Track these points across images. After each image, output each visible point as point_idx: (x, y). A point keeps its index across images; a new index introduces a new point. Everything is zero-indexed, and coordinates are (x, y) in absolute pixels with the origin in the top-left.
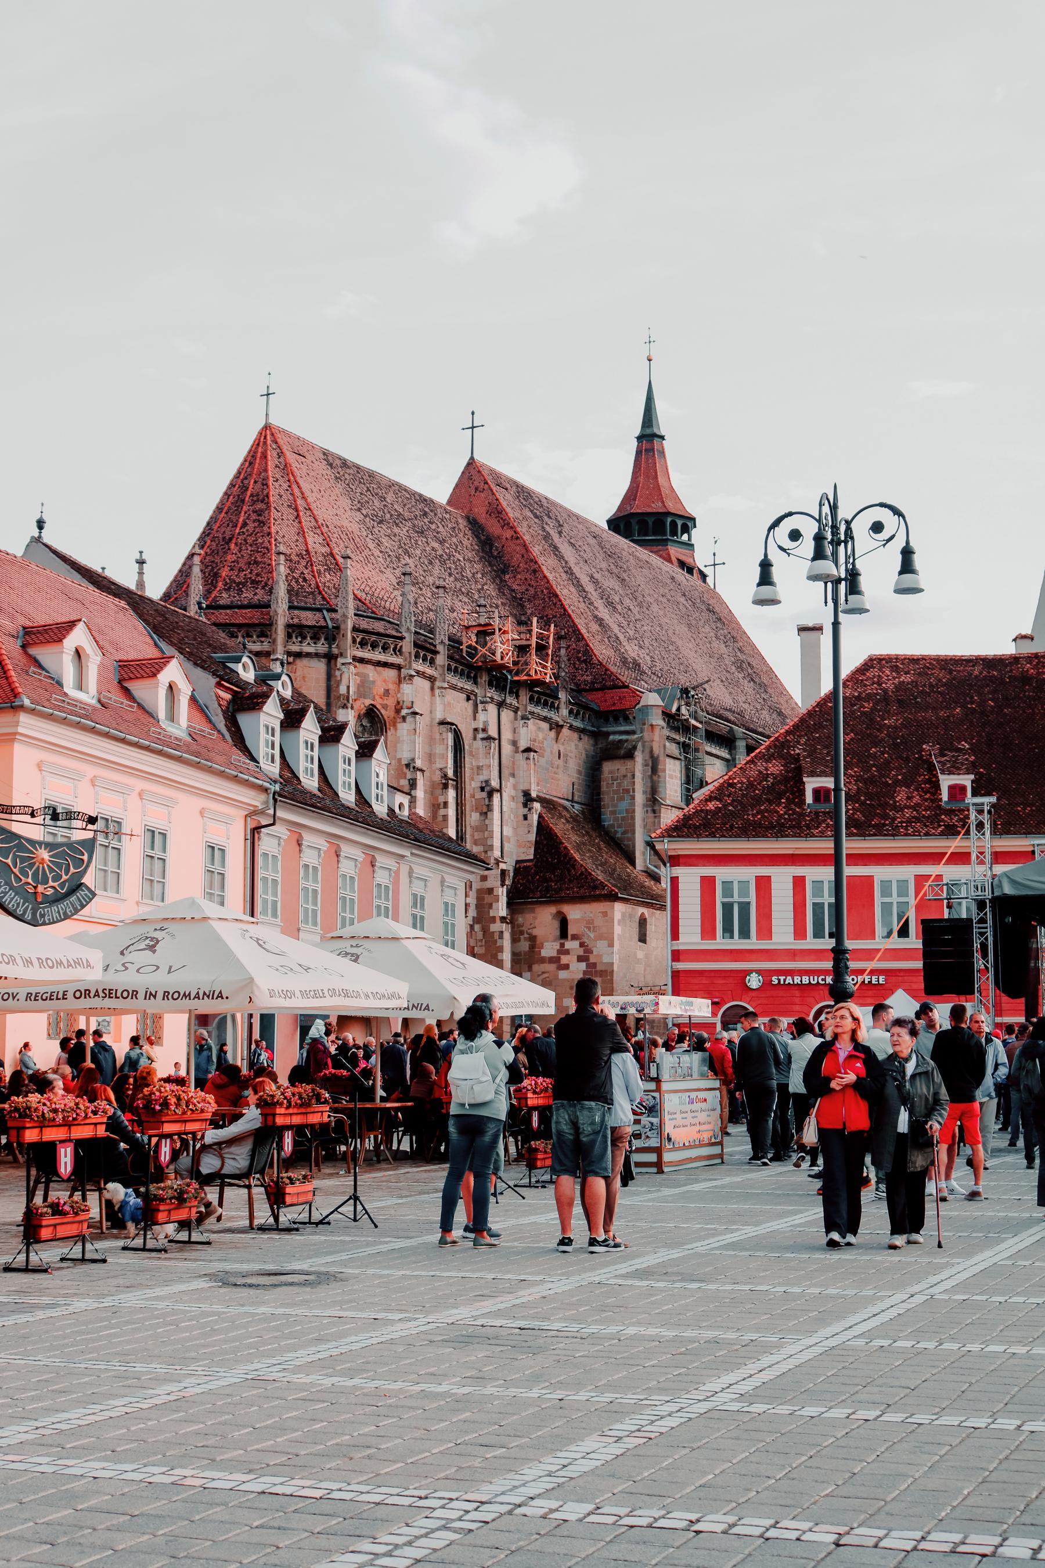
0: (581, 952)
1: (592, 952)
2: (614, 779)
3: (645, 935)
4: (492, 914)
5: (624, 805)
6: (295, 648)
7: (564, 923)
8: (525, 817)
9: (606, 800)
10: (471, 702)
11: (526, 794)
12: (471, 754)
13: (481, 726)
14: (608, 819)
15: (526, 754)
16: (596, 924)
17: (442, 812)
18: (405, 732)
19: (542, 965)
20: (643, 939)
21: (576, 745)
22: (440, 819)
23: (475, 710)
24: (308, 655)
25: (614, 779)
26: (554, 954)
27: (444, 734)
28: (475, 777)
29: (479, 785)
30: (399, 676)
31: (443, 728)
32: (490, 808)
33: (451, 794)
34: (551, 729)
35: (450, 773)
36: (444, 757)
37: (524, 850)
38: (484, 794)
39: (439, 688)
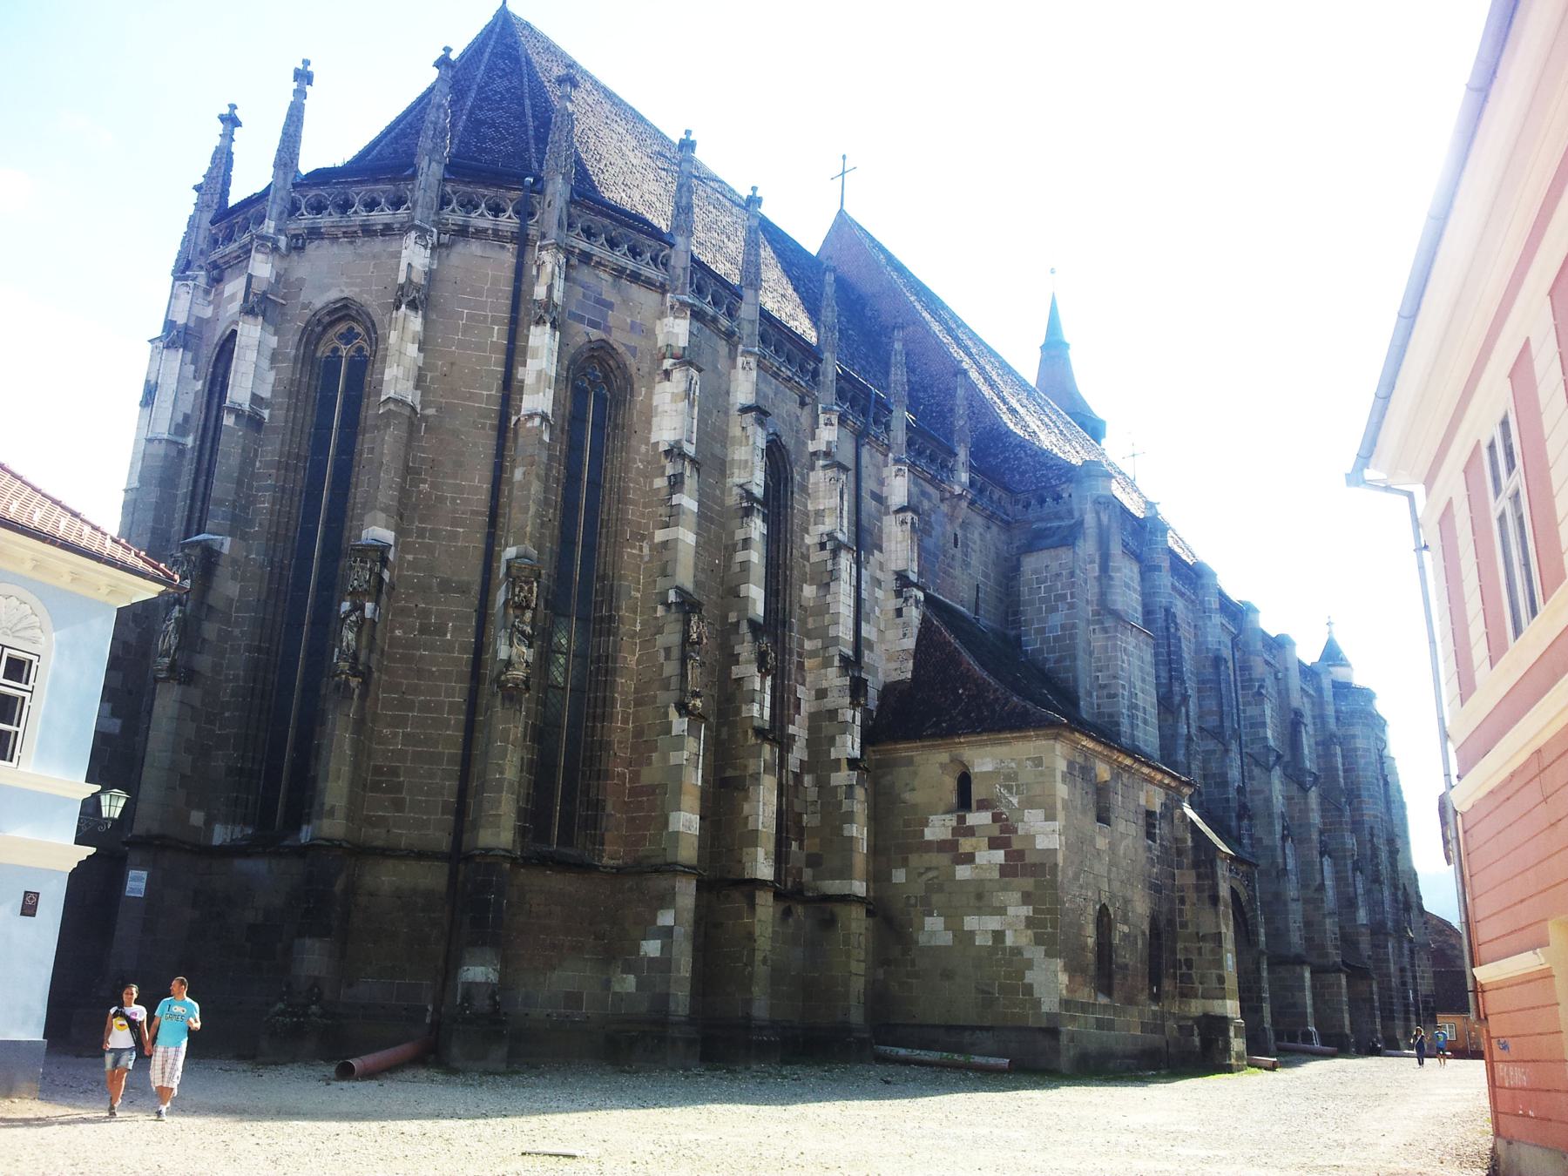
0: (995, 831)
1: (1015, 831)
2: (1039, 581)
3: (1108, 810)
5: (1057, 619)
6: (454, 217)
7: (964, 781)
8: (899, 613)
9: (1028, 612)
10: (807, 409)
11: (902, 577)
12: (804, 489)
14: (1032, 643)
15: (901, 516)
16: (1023, 779)
17: (740, 556)
18: (668, 398)
19: (926, 857)
20: (1103, 817)
21: (981, 534)
24: (480, 234)
25: (1039, 581)
26: (946, 835)
27: (750, 430)
28: (810, 528)
29: (816, 540)
30: (663, 303)
31: (750, 417)
32: (833, 576)
33: (757, 528)
34: (942, 500)
35: (758, 492)
38: (826, 554)
39: (747, 353)
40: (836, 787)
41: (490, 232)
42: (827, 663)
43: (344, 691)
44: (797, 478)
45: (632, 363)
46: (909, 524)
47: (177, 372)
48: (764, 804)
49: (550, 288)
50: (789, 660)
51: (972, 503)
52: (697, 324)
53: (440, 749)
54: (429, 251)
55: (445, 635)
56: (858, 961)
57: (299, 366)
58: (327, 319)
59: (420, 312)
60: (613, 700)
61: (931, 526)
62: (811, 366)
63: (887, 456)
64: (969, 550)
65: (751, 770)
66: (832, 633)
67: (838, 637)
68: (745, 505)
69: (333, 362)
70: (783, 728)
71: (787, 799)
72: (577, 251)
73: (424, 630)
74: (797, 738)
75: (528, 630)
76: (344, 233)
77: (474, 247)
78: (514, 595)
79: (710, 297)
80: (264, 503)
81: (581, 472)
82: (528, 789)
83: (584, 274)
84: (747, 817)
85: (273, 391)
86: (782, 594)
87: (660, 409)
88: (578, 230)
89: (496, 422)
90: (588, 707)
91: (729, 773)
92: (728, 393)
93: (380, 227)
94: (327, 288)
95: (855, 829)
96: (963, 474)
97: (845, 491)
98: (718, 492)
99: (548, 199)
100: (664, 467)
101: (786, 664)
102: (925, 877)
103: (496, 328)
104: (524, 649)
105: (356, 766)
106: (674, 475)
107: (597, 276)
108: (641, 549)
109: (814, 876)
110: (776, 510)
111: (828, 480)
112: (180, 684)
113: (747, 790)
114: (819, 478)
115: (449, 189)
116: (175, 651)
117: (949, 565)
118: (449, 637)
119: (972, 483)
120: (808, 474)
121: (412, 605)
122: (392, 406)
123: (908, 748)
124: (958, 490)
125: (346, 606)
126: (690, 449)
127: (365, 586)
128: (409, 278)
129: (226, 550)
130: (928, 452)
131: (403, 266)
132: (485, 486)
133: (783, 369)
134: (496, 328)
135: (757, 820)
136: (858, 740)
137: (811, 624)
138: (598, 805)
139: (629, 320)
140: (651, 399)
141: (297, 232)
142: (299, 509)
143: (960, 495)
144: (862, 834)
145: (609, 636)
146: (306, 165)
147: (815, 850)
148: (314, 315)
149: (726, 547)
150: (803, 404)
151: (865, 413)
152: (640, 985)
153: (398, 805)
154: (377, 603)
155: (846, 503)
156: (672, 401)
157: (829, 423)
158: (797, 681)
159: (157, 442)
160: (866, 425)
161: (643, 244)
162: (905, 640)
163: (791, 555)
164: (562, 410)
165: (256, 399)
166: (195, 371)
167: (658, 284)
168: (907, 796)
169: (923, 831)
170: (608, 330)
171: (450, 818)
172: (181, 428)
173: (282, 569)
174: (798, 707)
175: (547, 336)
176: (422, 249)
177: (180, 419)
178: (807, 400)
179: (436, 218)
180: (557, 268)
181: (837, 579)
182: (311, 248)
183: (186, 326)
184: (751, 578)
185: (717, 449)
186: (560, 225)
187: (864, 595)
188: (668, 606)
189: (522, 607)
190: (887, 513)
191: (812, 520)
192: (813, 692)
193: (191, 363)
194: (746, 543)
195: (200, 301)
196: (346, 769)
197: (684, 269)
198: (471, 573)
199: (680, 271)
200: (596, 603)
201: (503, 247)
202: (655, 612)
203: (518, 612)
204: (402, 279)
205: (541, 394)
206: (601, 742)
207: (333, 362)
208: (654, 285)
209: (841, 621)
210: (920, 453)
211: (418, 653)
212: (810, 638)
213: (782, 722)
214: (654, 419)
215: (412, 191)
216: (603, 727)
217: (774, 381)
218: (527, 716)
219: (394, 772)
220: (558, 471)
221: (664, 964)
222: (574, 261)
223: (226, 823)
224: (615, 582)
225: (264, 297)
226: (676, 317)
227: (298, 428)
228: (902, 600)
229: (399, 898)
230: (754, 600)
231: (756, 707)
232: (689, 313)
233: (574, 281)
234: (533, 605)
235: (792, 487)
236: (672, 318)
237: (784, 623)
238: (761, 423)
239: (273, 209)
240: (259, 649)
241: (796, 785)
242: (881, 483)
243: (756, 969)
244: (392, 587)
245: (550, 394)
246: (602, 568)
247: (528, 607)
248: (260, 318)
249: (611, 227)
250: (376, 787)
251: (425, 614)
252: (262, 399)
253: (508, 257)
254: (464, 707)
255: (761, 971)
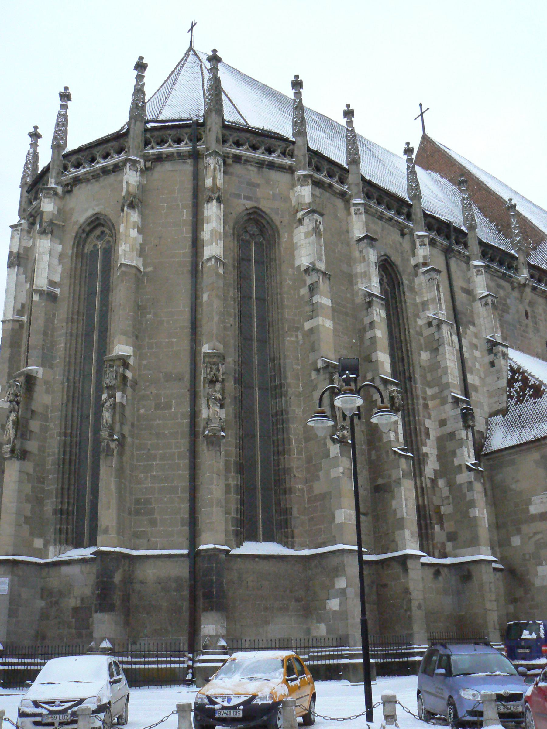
4: (456, 462)
8: (492, 364)
10: (407, 237)
12: (412, 289)
13: (422, 261)
17: (369, 335)
18: (303, 236)
22: (367, 343)
23: (414, 247)
24: (169, 157)
27: (365, 251)
28: (421, 314)
29: (425, 321)
30: (293, 179)
34: (513, 289)
36: (366, 275)
37: (496, 399)
40: (461, 485)
41: (175, 154)
42: (444, 402)
43: (109, 452)
44: (406, 282)
45: (277, 219)
46: (490, 305)
47: (15, 279)
48: (406, 500)
49: (214, 178)
50: (417, 403)
51: (534, 289)
52: (318, 191)
53: (175, 483)
54: (139, 173)
55: (171, 408)
56: (491, 601)
57: (74, 259)
58: (88, 229)
59: (136, 210)
60: (289, 439)
61: (508, 307)
62: (405, 210)
63: (468, 263)
64: (537, 320)
65: (394, 477)
66: (444, 380)
67: (448, 384)
68: (368, 300)
69: (94, 254)
70: (418, 450)
71: (428, 498)
72: (231, 155)
73: (158, 407)
74: (429, 455)
75: (219, 396)
76: (93, 176)
77: (167, 167)
78: (207, 374)
79: (325, 173)
80: (60, 344)
81: (251, 293)
82: (237, 503)
83: (238, 169)
84: (395, 510)
85: (61, 277)
86: (406, 361)
87: (298, 245)
88: (230, 142)
89: (189, 268)
90: (274, 447)
91: (380, 481)
92: (347, 231)
93: (111, 167)
94: (87, 210)
95: (477, 511)
96: (524, 271)
97: (440, 285)
98: (349, 295)
99: (208, 128)
100: (305, 281)
101: (415, 406)
102: (533, 540)
103: (185, 211)
104: (217, 409)
105: (121, 499)
106: (312, 284)
107: (247, 169)
108: (297, 337)
109: (453, 546)
110: (394, 306)
111: (427, 281)
112: (18, 460)
113: (392, 492)
114: (421, 280)
115: (148, 136)
116: (14, 441)
117: (524, 331)
118: (173, 410)
119: (532, 276)
120: (414, 280)
121: (149, 392)
122: (123, 269)
123: (511, 454)
124: (523, 282)
125: (104, 396)
126: (321, 266)
127: (114, 382)
128: (128, 192)
129: (40, 375)
130: (498, 259)
131: (125, 185)
132: (187, 309)
133: (385, 212)
134: (185, 211)
135: (402, 511)
136: (472, 451)
137: (429, 377)
138: (287, 512)
139: (271, 193)
140: (292, 240)
141: (67, 182)
142: (82, 345)
143: (525, 285)
144: (483, 514)
145: (281, 397)
146: (72, 144)
147: (452, 529)
148: (80, 227)
149: (359, 331)
150: (403, 235)
151: (448, 237)
152: (328, 632)
153: (153, 523)
154: (124, 392)
155: (442, 294)
156: (305, 238)
157: (422, 244)
158: (424, 417)
159: (7, 322)
160: (450, 243)
161: (275, 146)
162: (499, 382)
163: (409, 332)
164: (232, 254)
165: (51, 283)
166: (26, 277)
167: (287, 167)
168: (513, 486)
169: (528, 509)
170: (257, 200)
171: (186, 529)
172: (20, 312)
173: (74, 383)
174: (428, 434)
175: (214, 208)
176: (135, 173)
177: (19, 307)
178: (406, 231)
179: (142, 154)
180: (218, 167)
181: (443, 344)
182: (75, 190)
183: (18, 253)
184: (378, 347)
185: (345, 268)
186: (217, 141)
187: (466, 355)
188: (318, 370)
189: (213, 382)
190: (474, 300)
191: (421, 308)
192: (437, 423)
193: (24, 273)
194: (372, 325)
195: (25, 237)
196: (114, 502)
197: (304, 155)
198: (184, 367)
199: (301, 158)
200: (271, 377)
201: (184, 163)
202: (310, 376)
203: (212, 385)
204: (124, 193)
205: (214, 244)
206: (284, 469)
207: (94, 254)
208: (285, 169)
209: (449, 371)
210: (492, 260)
211: (156, 423)
212: (430, 387)
213: (417, 446)
214: (296, 252)
215: (127, 142)
216: (284, 458)
217: (380, 222)
218: (226, 455)
219: (148, 501)
220: (232, 293)
221: (343, 615)
222: (230, 161)
223: (55, 544)
224: (282, 361)
225: (51, 223)
226: (302, 186)
227: (77, 296)
228: (493, 355)
229: (160, 583)
230: (383, 363)
231: (392, 434)
232: (310, 181)
233: (232, 174)
234: (220, 379)
235: (403, 289)
236: (299, 187)
237: (410, 379)
238: (373, 247)
239: (53, 173)
240: (65, 435)
241: (433, 487)
242: (469, 281)
243: (413, 612)
244: (135, 383)
245: (221, 243)
246: (272, 353)
247: (217, 381)
248: (50, 235)
249: (252, 138)
250: (138, 513)
251: (158, 396)
252: (56, 283)
253: (188, 167)
254: (188, 454)
255: (417, 614)
